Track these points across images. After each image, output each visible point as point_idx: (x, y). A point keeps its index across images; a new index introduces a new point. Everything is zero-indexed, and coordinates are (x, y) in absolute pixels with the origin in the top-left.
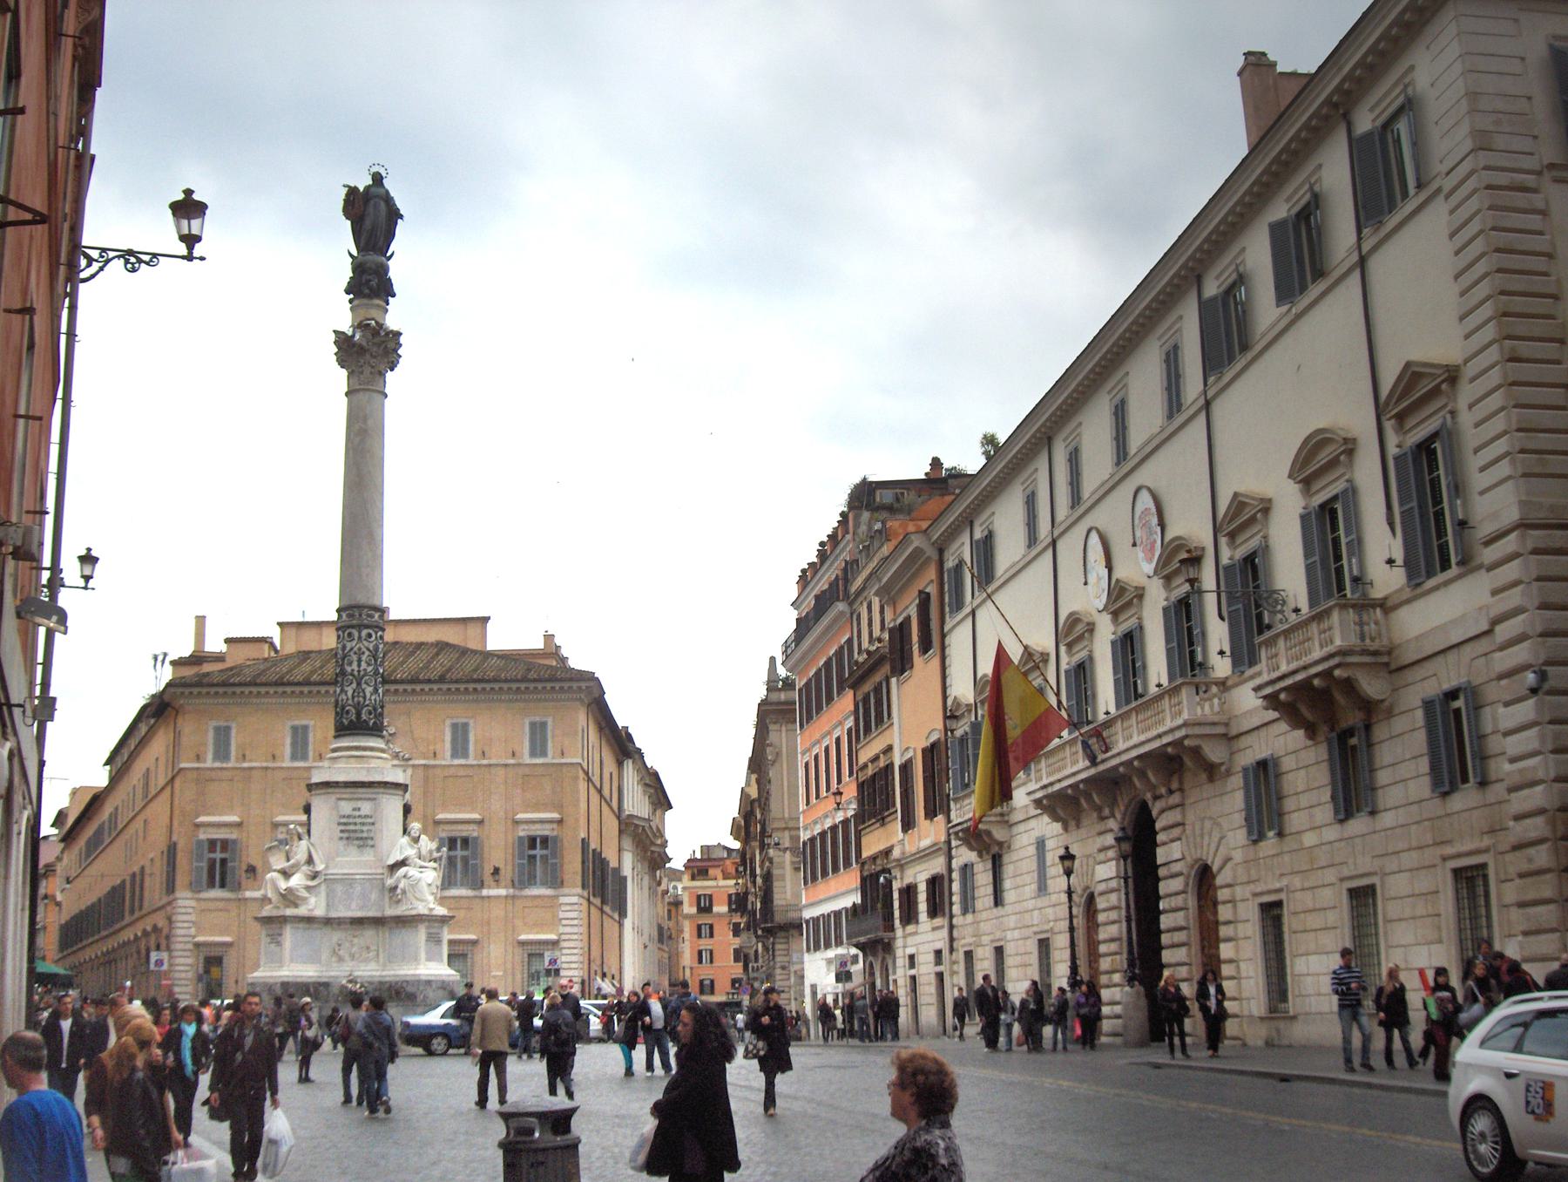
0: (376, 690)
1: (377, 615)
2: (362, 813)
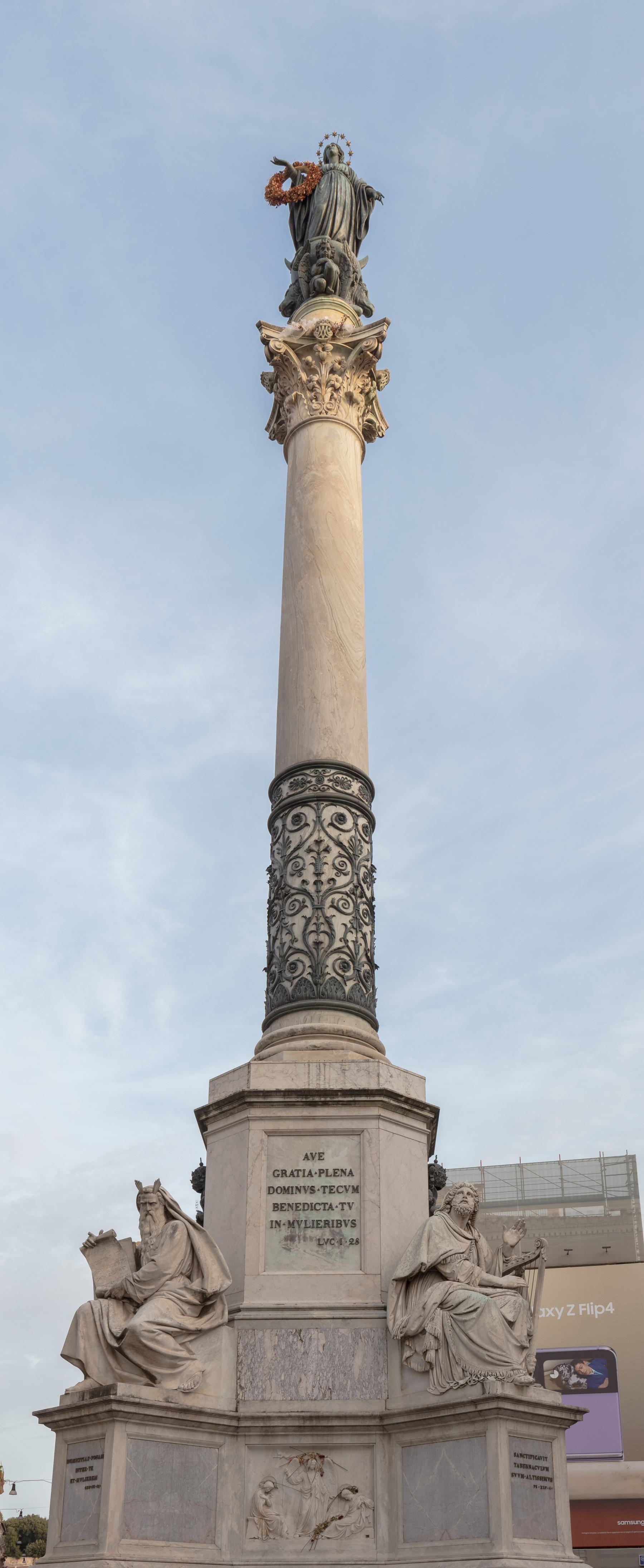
0: (356, 926)
1: (356, 787)
2: (329, 1163)
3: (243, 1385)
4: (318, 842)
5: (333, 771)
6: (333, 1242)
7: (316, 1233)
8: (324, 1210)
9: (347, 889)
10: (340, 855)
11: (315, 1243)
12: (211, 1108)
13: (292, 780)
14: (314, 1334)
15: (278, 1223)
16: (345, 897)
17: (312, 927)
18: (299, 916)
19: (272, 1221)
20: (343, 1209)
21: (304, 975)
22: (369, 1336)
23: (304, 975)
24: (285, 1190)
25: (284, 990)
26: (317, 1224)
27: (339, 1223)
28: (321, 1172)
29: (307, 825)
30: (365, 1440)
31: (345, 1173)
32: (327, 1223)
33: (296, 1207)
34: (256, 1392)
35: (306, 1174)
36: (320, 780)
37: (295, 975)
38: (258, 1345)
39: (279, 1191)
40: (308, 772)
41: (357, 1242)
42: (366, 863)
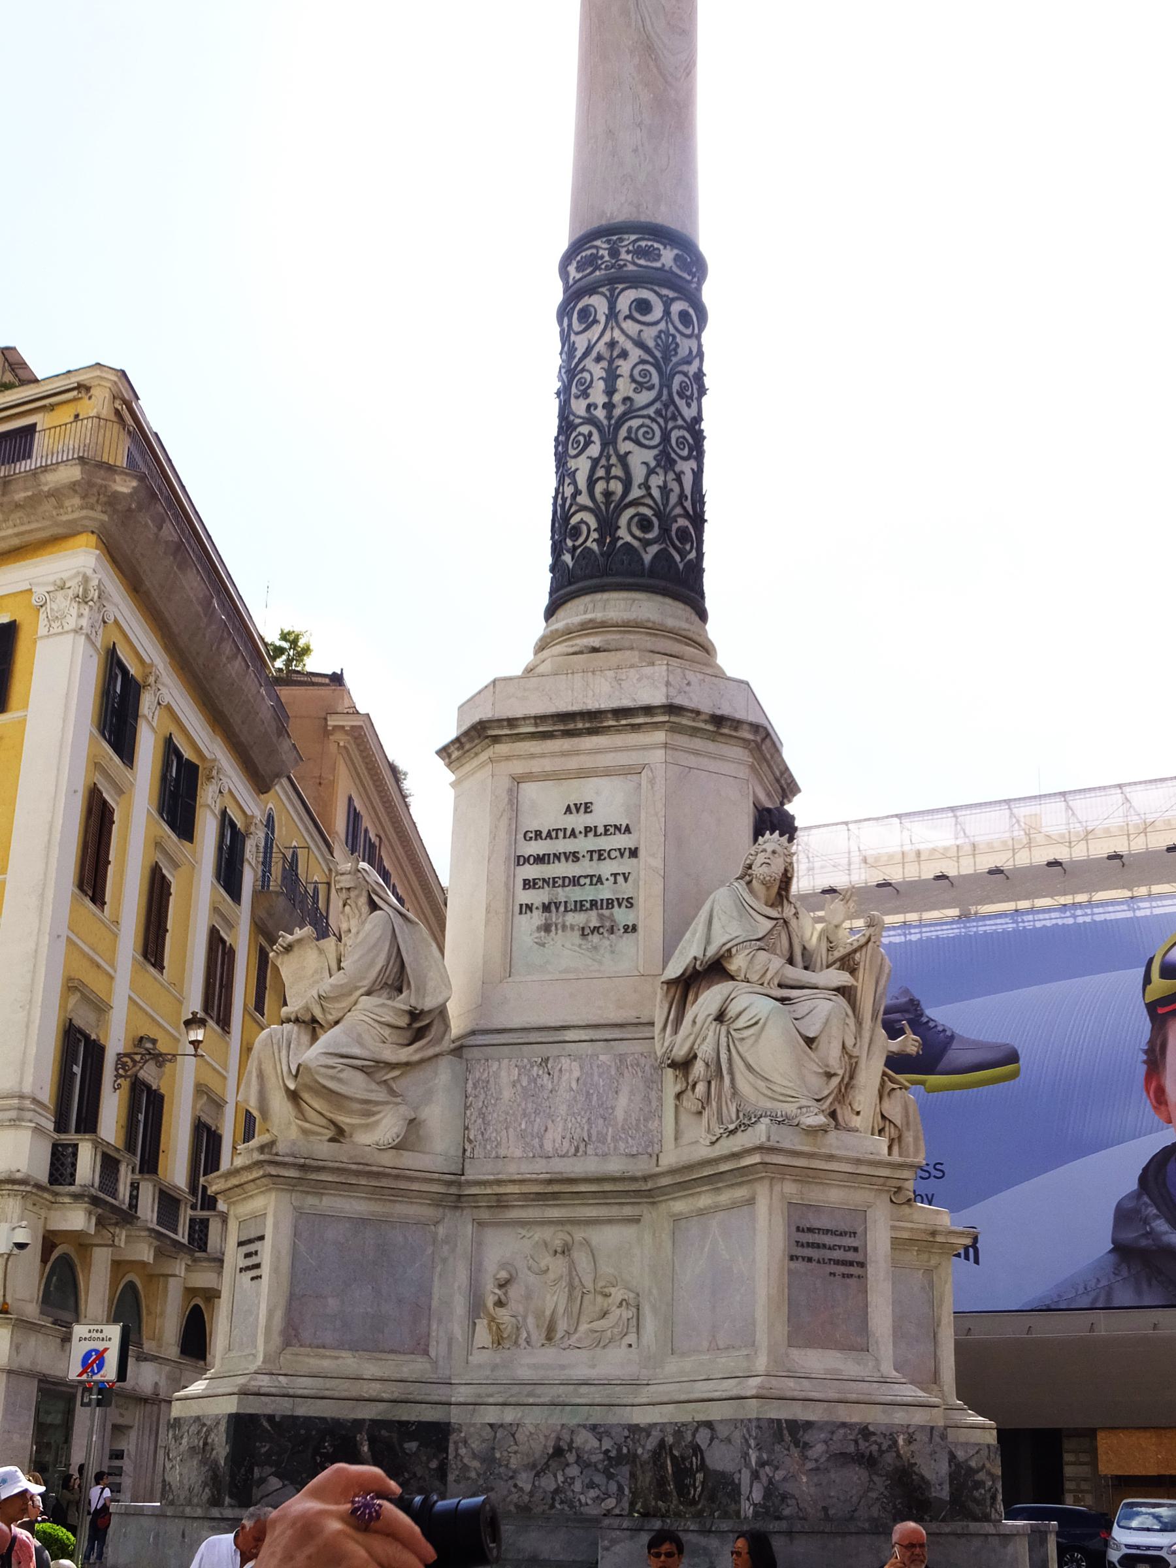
0: (666, 461)
1: (668, 256)
2: (597, 819)
3: (472, 1137)
4: (612, 344)
5: (633, 237)
6: (601, 930)
7: (578, 919)
8: (591, 884)
9: (651, 411)
10: (643, 362)
11: (577, 933)
12: (452, 748)
13: (579, 258)
14: (565, 1062)
15: (529, 907)
16: (647, 421)
17: (601, 473)
18: (584, 456)
19: (521, 905)
20: (615, 882)
21: (588, 544)
22: (638, 1065)
23: (588, 544)
24: (540, 859)
25: (565, 564)
26: (580, 906)
27: (610, 903)
28: (587, 830)
29: (595, 321)
30: (628, 1211)
31: (620, 830)
32: (593, 904)
33: (551, 882)
34: (488, 1147)
35: (568, 833)
36: (614, 253)
37: (577, 543)
38: (492, 1080)
39: (532, 861)
40: (598, 243)
41: (634, 928)
42: (685, 368)
